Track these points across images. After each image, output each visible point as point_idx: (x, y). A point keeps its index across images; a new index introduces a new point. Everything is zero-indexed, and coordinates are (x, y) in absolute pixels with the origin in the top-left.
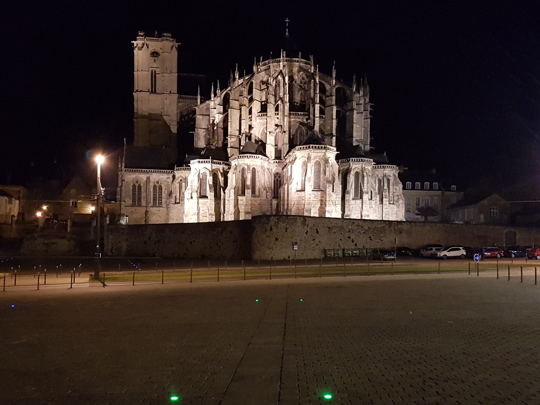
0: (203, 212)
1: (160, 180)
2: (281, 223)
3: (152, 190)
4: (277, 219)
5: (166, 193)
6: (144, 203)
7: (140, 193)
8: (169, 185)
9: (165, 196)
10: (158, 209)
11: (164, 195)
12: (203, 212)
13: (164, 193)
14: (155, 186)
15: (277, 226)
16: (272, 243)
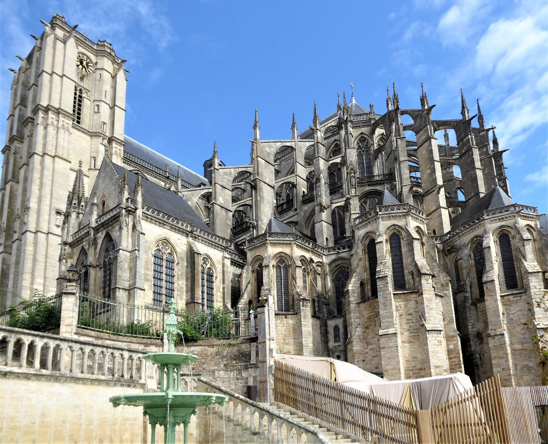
1: (209, 257)
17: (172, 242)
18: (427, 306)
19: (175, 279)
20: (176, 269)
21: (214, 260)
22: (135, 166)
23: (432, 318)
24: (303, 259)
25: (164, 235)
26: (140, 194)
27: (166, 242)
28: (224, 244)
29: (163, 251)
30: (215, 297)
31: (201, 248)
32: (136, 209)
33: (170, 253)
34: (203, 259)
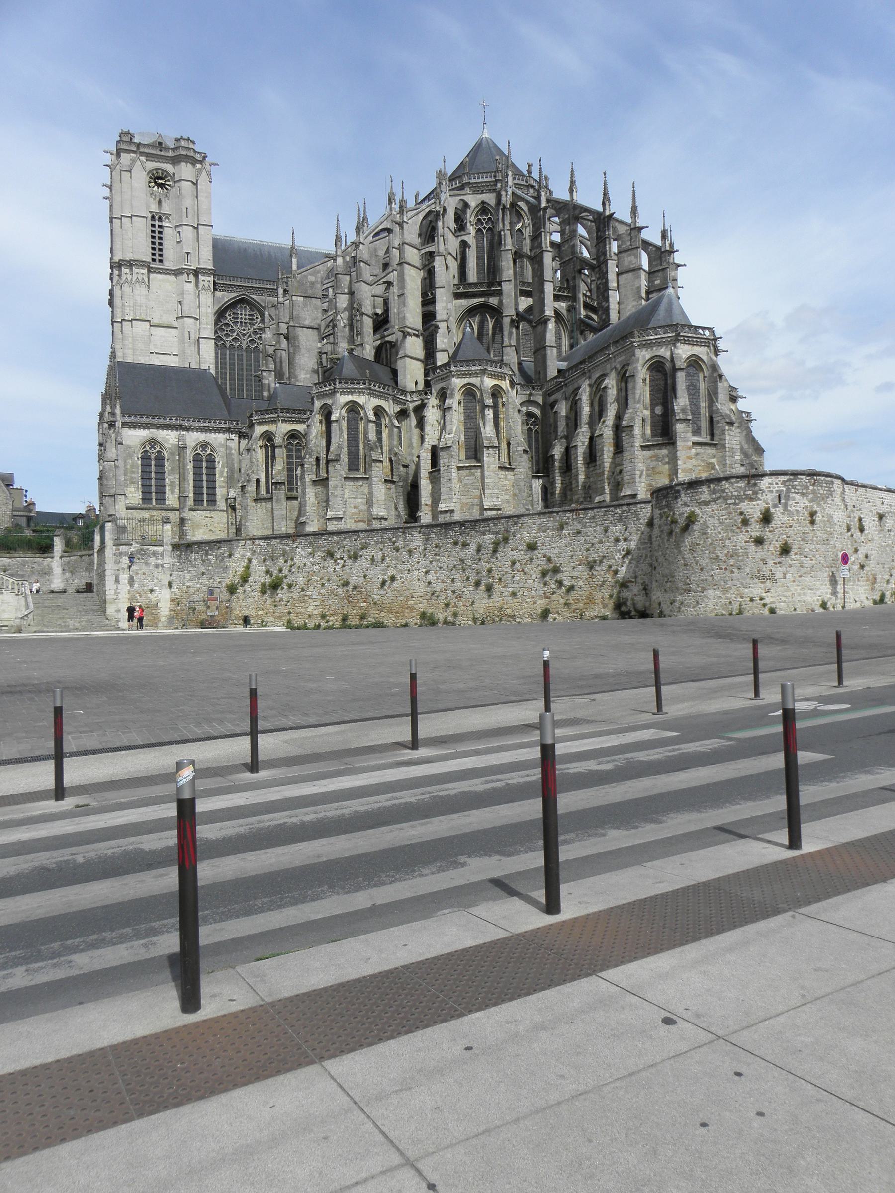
0: (354, 510)
1: (208, 444)
2: (797, 496)
3: (190, 466)
4: (784, 483)
5: (225, 474)
6: (171, 499)
7: (161, 474)
8: (233, 454)
9: (223, 482)
10: (208, 514)
11: (220, 480)
12: (354, 510)
13: (221, 476)
14: (197, 459)
15: (786, 505)
16: (771, 563)
17: (160, 440)
18: (332, 493)
19: (166, 474)
20: (166, 465)
21: (214, 445)
22: (238, 290)
23: (335, 506)
24: (293, 435)
25: (151, 436)
26: (118, 407)
27: (153, 442)
28: (227, 426)
29: (150, 451)
30: (218, 484)
31: (193, 438)
32: (115, 422)
33: (158, 452)
34: (201, 446)
